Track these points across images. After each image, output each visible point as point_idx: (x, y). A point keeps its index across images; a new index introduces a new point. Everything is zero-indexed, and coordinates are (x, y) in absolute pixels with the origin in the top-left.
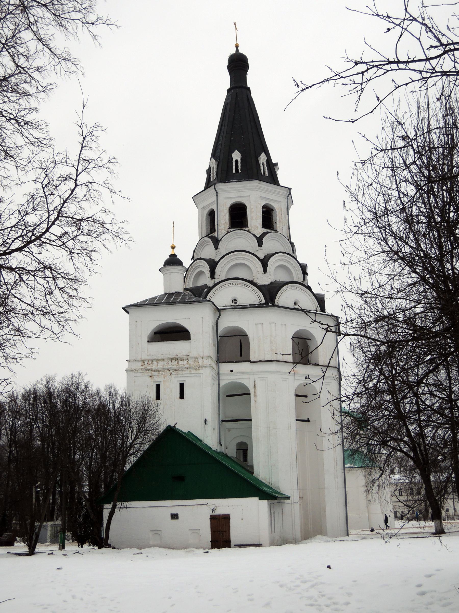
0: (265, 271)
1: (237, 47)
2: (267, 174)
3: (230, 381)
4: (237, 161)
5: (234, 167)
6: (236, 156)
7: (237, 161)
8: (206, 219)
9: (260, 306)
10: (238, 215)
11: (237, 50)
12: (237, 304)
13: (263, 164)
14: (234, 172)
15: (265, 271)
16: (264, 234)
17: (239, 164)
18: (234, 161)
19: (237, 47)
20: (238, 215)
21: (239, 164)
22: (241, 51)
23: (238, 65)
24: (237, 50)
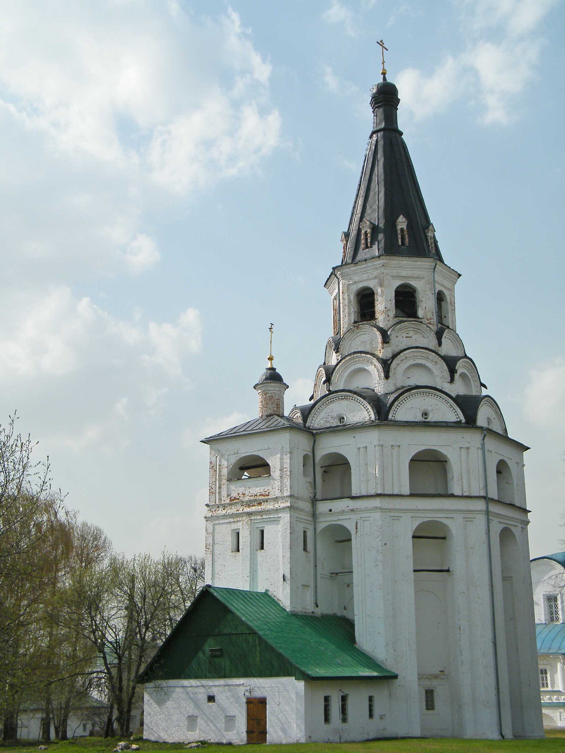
0: (452, 380)
1: (384, 74)
3: (426, 520)
5: (399, 236)
6: (402, 223)
9: (457, 425)
10: (406, 300)
11: (385, 79)
12: (427, 420)
14: (400, 244)
15: (452, 380)
17: (406, 233)
18: (399, 227)
19: (384, 74)
20: (406, 300)
21: (406, 233)
22: (389, 80)
23: (386, 98)
24: (385, 79)
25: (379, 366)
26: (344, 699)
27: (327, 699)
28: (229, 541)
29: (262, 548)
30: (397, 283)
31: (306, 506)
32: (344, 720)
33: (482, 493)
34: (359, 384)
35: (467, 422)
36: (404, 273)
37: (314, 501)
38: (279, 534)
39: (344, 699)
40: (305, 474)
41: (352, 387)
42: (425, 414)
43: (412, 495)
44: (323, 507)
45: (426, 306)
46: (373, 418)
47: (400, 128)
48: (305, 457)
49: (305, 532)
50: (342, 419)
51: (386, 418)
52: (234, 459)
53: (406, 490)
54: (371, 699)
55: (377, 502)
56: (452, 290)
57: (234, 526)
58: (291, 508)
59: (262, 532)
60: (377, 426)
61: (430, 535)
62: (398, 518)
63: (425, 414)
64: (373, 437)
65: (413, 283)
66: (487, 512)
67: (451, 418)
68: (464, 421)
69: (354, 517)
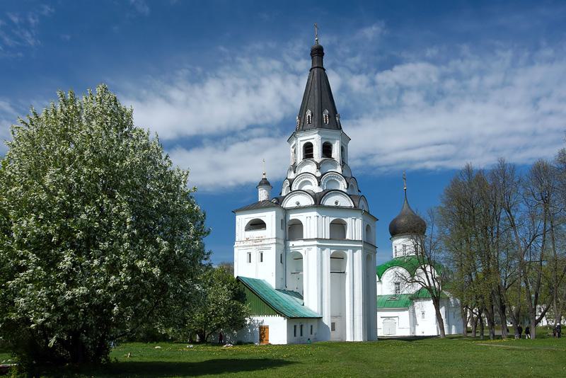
10: (327, 150)
25: (316, 180)
26: (301, 326)
27: (295, 326)
28: (246, 257)
29: (262, 261)
31: (282, 242)
32: (301, 335)
34: (306, 188)
35: (355, 207)
36: (327, 137)
37: (286, 241)
38: (271, 255)
39: (301, 326)
40: (282, 228)
41: (302, 189)
42: (336, 203)
44: (291, 243)
45: (336, 153)
46: (313, 203)
47: (324, 67)
48: (282, 220)
50: (298, 203)
52: (248, 221)
53: (328, 237)
54: (311, 326)
55: (316, 243)
56: (347, 146)
57: (249, 251)
59: (262, 254)
60: (317, 207)
61: (338, 259)
62: (324, 250)
63: (336, 203)
64: (314, 214)
65: (331, 142)
69: (305, 248)
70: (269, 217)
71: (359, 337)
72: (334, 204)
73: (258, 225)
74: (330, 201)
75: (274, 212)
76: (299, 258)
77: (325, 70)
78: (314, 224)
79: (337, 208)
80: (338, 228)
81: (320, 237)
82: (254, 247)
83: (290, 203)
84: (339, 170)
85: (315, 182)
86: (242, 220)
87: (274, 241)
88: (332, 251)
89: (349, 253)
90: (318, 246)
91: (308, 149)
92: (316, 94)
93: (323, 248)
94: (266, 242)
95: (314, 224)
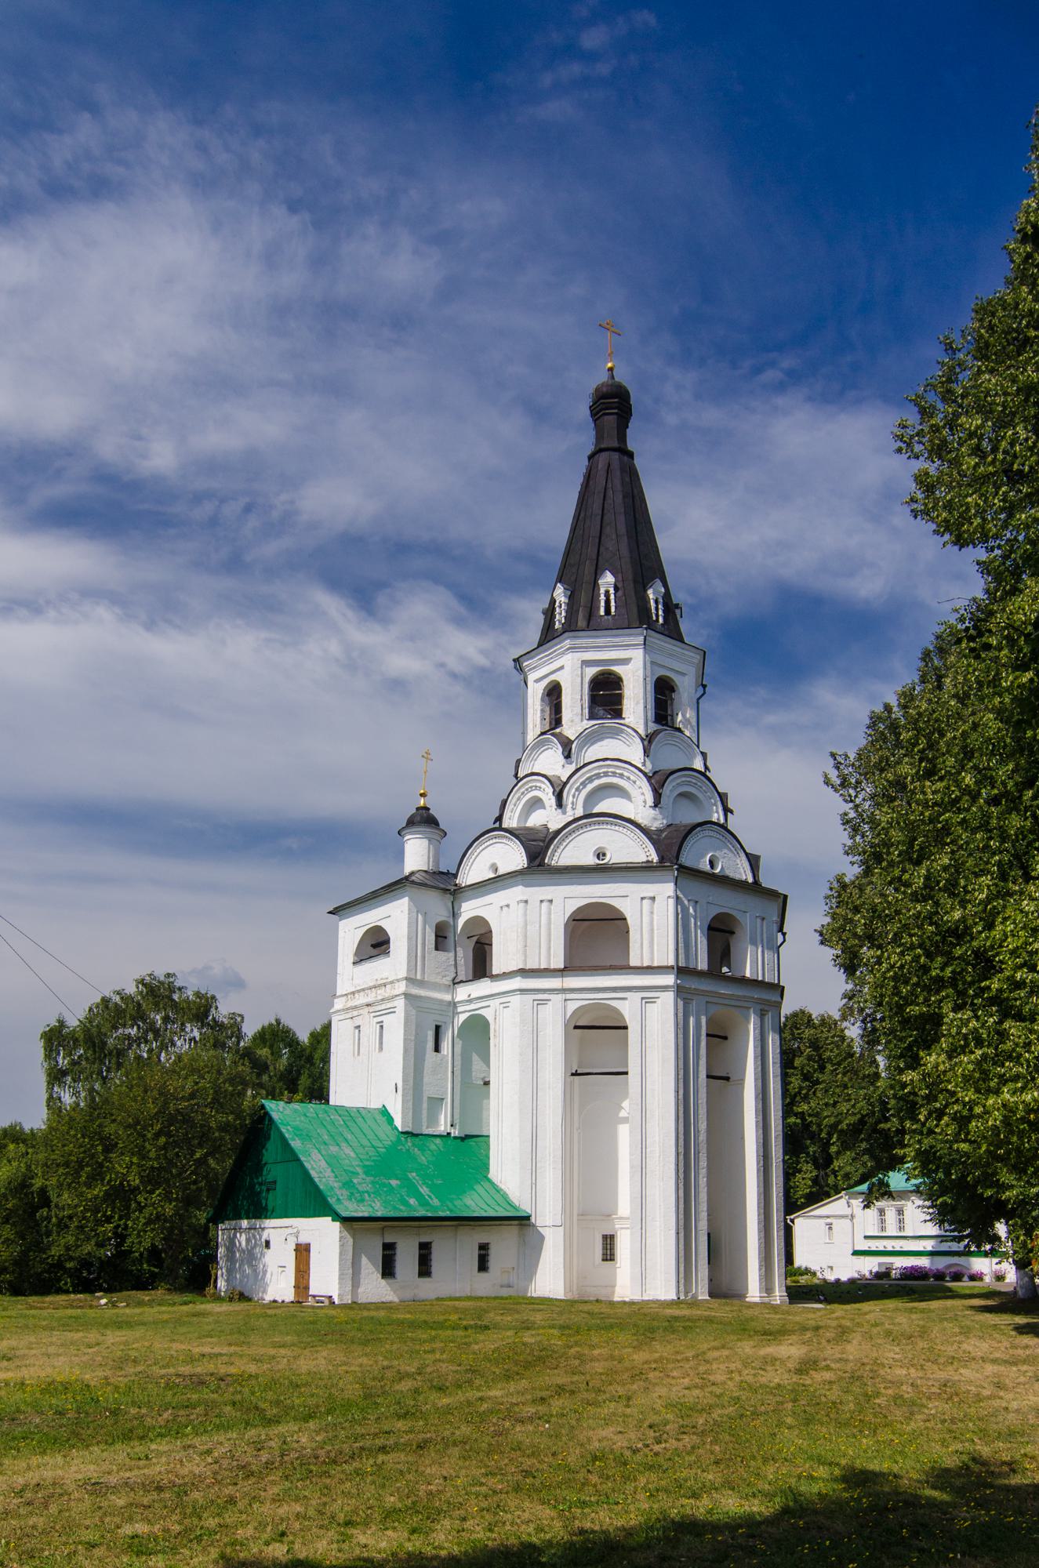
2: (661, 620)
4: (607, 593)
5: (603, 604)
7: (607, 593)
8: (542, 700)
10: (605, 694)
13: (656, 602)
14: (602, 612)
16: (655, 733)
17: (612, 597)
18: (602, 591)
20: (605, 694)
21: (612, 597)
29: (381, 1048)
30: (591, 672)
32: (425, 1269)
33: (671, 962)
42: (600, 854)
43: (567, 970)
47: (631, 446)
49: (438, 1028)
51: (542, 864)
53: (558, 962)
54: (484, 1247)
55: (517, 983)
58: (406, 995)
62: (543, 1002)
63: (600, 854)
64: (516, 893)
66: (680, 991)
67: (641, 858)
68: (655, 858)
69: (494, 1003)
70: (396, 917)
71: (662, 1288)
72: (590, 860)
73: (376, 944)
74: (574, 852)
75: (406, 900)
76: (478, 1031)
77: (631, 455)
78: (526, 923)
79: (602, 870)
80: (596, 937)
81: (532, 964)
82: (367, 1009)
83: (474, 872)
84: (634, 752)
85: (548, 796)
86: (351, 930)
87: (401, 987)
88: (573, 1006)
89: (628, 1008)
90: (523, 991)
91: (554, 693)
92: (622, 529)
93: (540, 996)
94: (387, 992)
95: (526, 923)
